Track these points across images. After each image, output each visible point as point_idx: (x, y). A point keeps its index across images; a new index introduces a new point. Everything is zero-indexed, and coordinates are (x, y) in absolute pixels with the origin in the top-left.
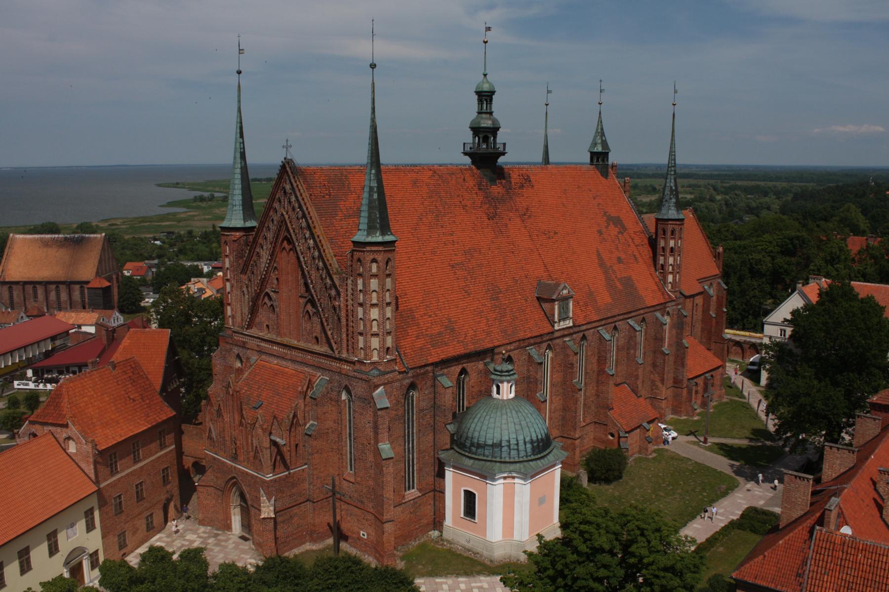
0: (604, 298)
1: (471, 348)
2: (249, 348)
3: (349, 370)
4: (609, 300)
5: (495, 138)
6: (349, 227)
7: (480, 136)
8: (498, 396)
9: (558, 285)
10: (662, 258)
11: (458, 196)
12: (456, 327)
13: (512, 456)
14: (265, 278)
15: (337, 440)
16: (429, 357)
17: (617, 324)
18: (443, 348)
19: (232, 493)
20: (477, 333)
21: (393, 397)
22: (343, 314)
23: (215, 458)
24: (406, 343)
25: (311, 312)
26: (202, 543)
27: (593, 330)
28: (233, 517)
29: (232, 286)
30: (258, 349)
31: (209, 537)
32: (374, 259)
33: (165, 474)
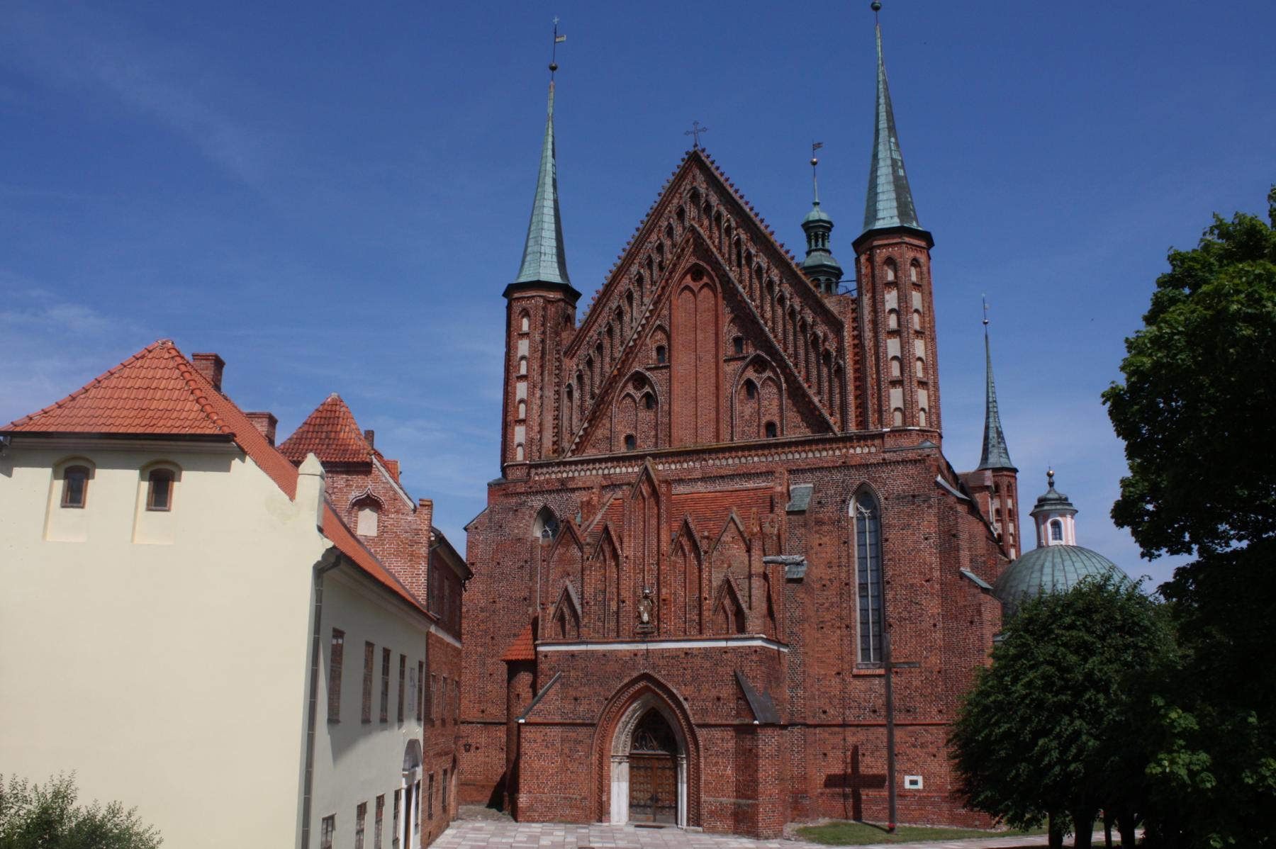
14: (635, 345)
19: (620, 724)
23: (573, 655)
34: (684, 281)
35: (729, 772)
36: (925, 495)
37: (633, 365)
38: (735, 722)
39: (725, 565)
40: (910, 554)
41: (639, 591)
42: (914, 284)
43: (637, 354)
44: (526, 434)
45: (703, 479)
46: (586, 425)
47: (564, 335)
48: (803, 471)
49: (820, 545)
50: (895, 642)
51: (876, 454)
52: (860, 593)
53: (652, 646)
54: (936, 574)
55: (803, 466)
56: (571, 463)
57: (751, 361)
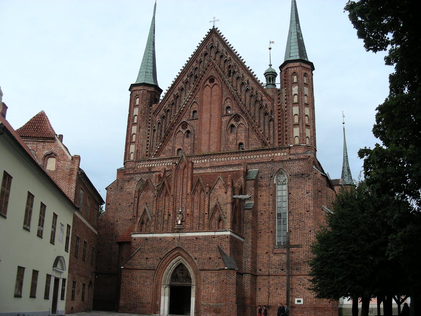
2: (154, 172)
19: (166, 270)
23: (146, 239)
28: (162, 298)
32: (306, 73)
34: (206, 83)
35: (213, 291)
36: (308, 174)
37: (183, 119)
38: (217, 269)
39: (216, 199)
40: (300, 199)
41: (177, 210)
42: (305, 84)
43: (184, 114)
44: (135, 148)
45: (210, 167)
46: (161, 144)
47: (154, 106)
48: (254, 164)
49: (261, 196)
50: (293, 238)
51: (286, 156)
52: (278, 217)
53: (182, 235)
54: (312, 208)
55: (254, 161)
56: (153, 160)
57: (235, 116)
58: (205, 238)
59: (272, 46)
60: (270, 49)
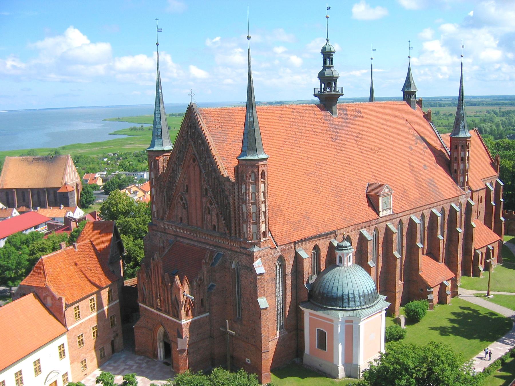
0: (414, 194)
1: (321, 231)
2: (167, 233)
3: (237, 247)
4: (418, 195)
5: (335, 84)
6: (235, 149)
7: (325, 83)
8: (340, 264)
9: (381, 186)
10: (455, 165)
11: (311, 125)
12: (310, 216)
13: (350, 306)
15: (229, 295)
16: (292, 238)
17: (424, 211)
18: (301, 231)
20: (325, 220)
21: (267, 266)
22: (232, 209)
23: (146, 309)
24: (276, 228)
25: (210, 208)
26: (137, 367)
27: (407, 216)
29: (156, 191)
30: (174, 234)
31: (142, 363)
33: (113, 320)
58: (172, 321)
59: (329, 13)
60: (327, 18)
